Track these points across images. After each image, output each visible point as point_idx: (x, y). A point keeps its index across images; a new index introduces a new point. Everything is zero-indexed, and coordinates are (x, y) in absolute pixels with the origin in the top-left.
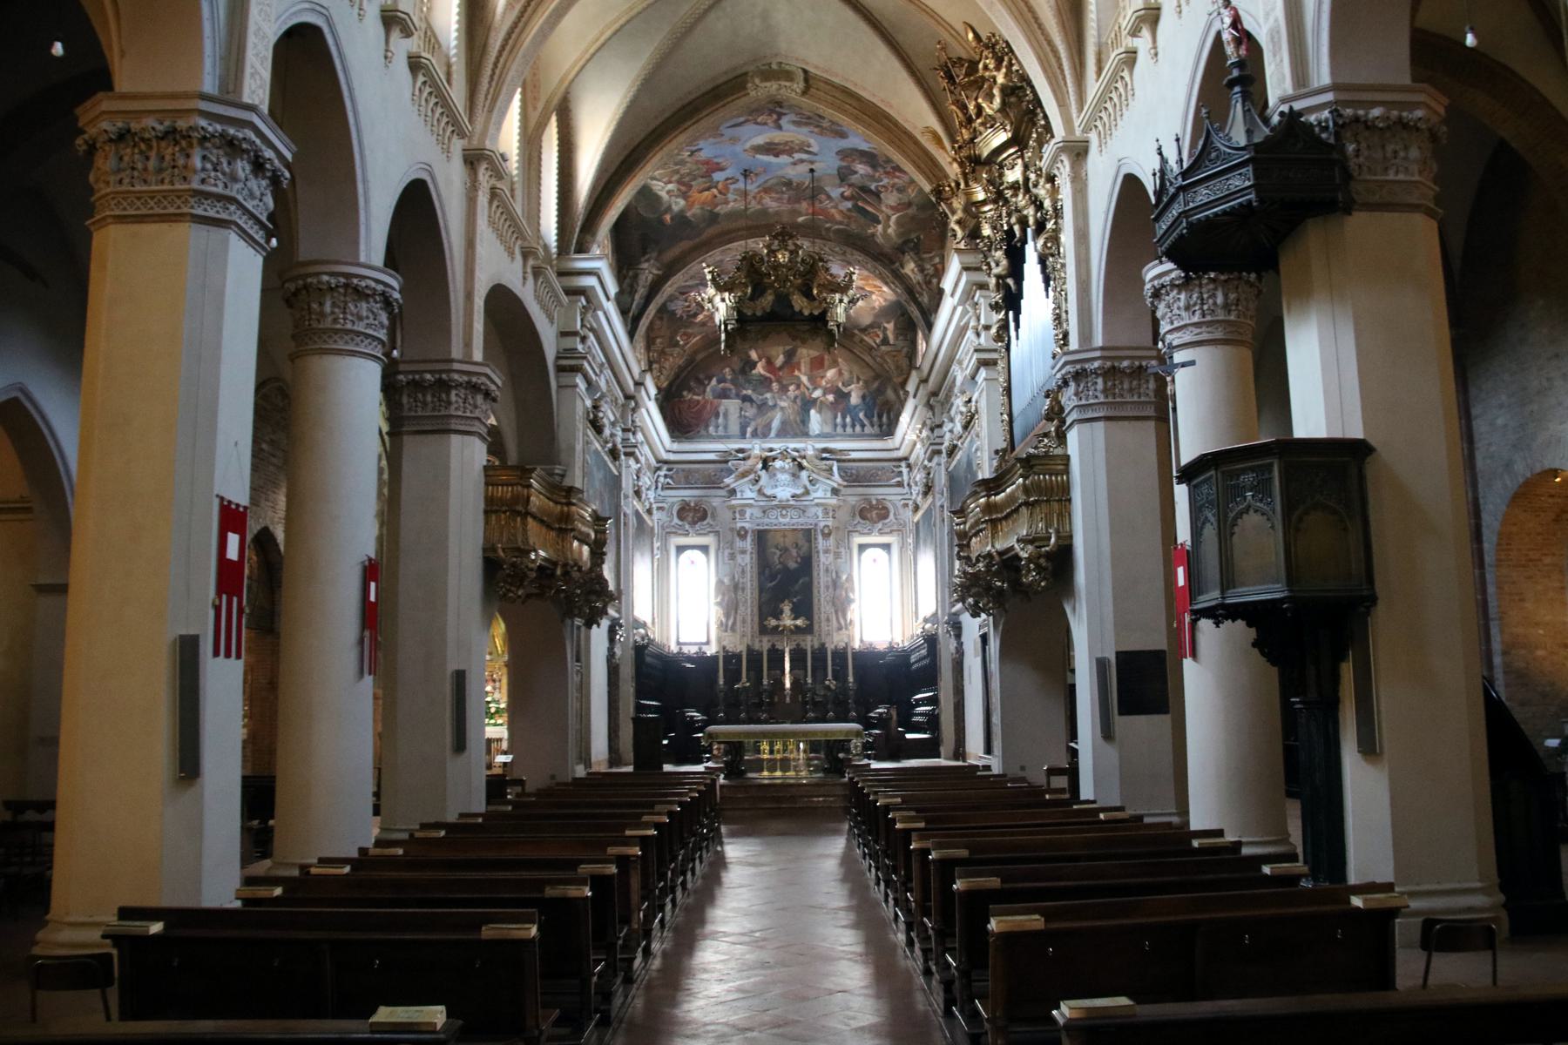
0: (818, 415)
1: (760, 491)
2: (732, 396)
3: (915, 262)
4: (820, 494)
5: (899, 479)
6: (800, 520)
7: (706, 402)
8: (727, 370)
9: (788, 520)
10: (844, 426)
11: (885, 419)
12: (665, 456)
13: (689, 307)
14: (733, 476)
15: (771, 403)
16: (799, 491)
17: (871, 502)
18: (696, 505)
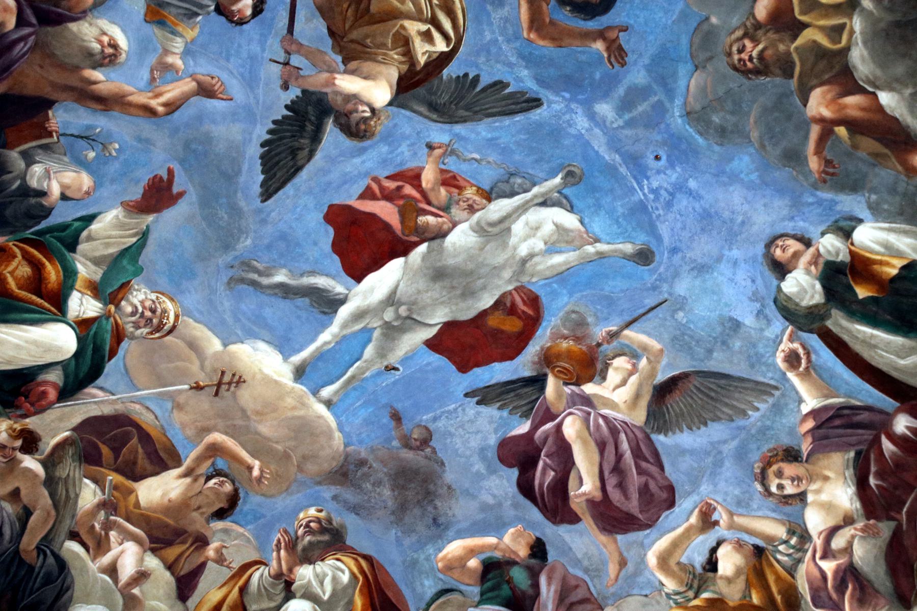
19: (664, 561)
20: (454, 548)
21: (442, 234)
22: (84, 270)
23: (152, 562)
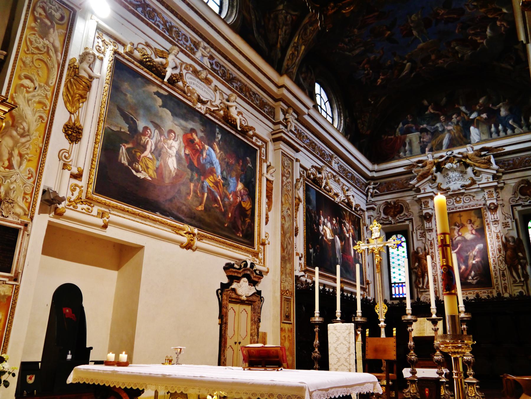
0: (476, 130)
2: (413, 131)
4: (484, 181)
7: (397, 138)
8: (409, 116)
9: (461, 204)
10: (498, 132)
12: (370, 174)
13: (368, 74)
14: (416, 179)
15: (440, 129)
16: (468, 182)
18: (395, 203)
19: (470, 9)
20: (457, 31)
21: (411, 27)
22: (400, 62)
23: (443, 59)
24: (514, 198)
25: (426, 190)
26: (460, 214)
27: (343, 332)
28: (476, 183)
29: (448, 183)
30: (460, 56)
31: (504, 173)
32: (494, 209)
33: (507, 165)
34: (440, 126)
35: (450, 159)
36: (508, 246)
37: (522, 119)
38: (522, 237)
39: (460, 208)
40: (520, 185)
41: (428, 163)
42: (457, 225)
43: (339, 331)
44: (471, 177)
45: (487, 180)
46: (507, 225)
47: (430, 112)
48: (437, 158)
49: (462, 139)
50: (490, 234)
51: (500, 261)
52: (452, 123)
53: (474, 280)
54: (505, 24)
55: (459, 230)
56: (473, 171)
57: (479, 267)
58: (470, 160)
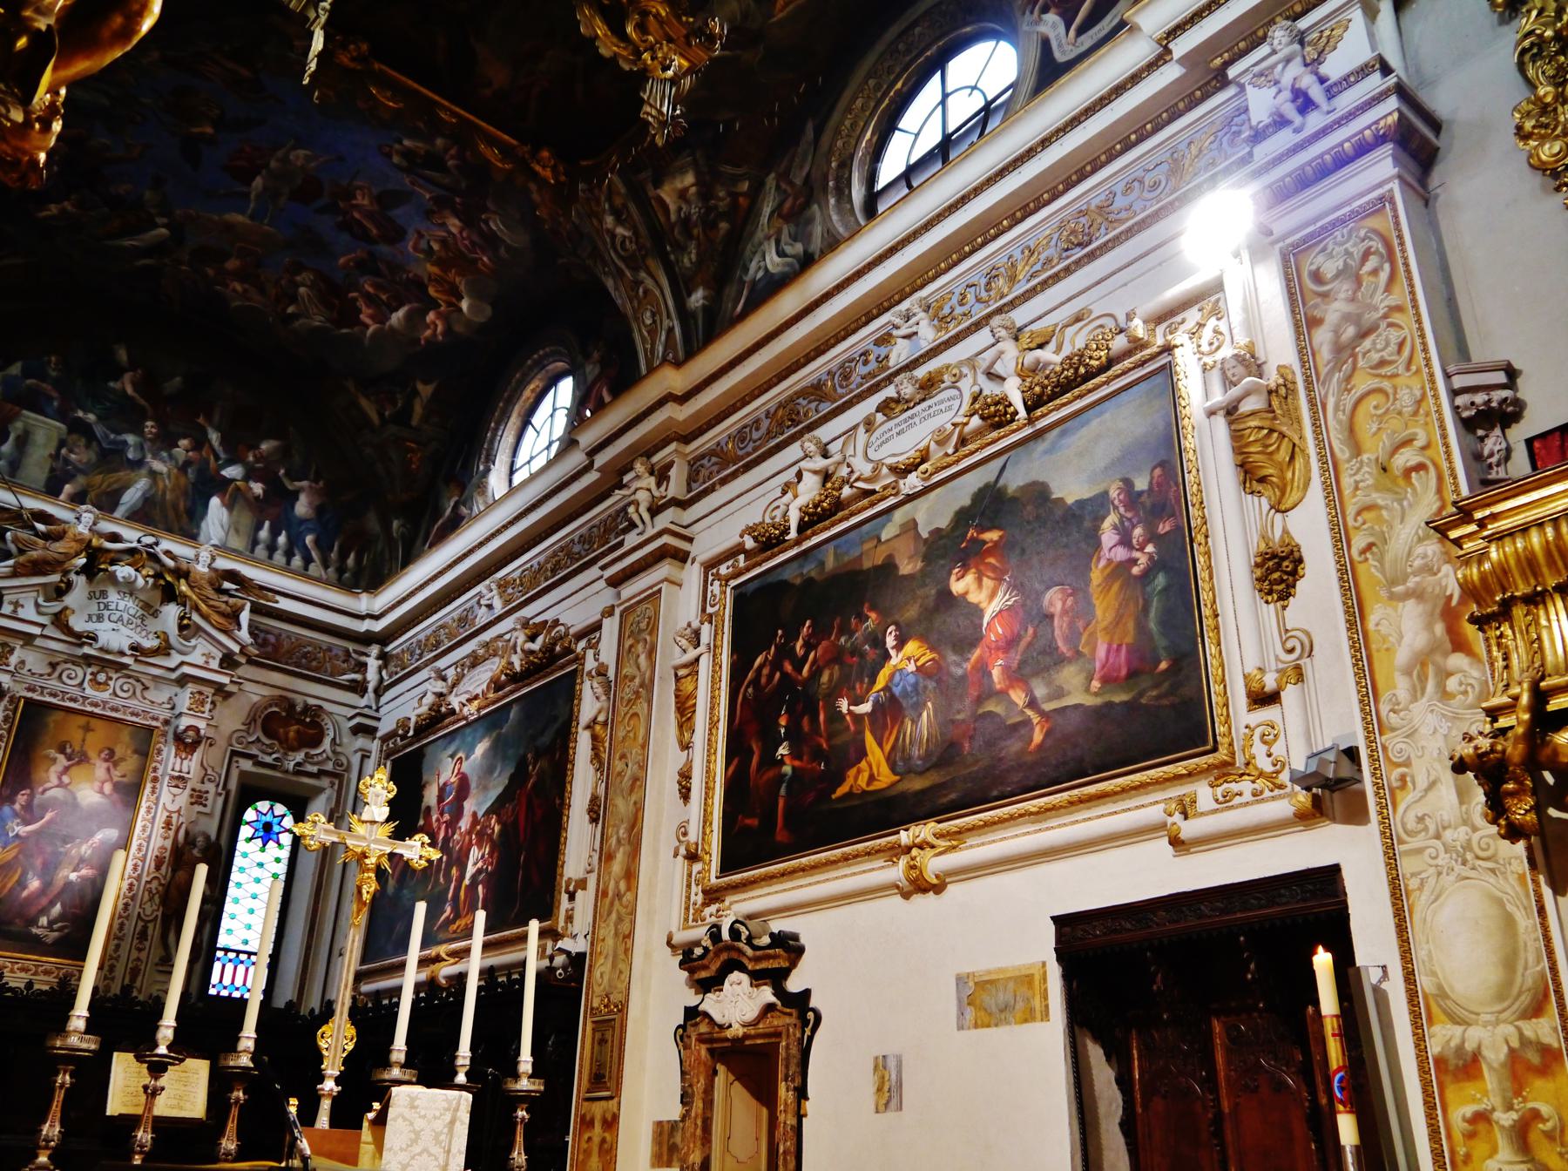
0: (224, 512)
1: (60, 620)
3: (698, 175)
4: (196, 657)
5: (358, 677)
6: (133, 703)
9: (106, 695)
10: (272, 548)
11: (351, 561)
14: (11, 562)
15: (130, 455)
16: (150, 643)
17: (291, 705)
19: (415, 248)
20: (342, 261)
22: (153, 211)
23: (246, 286)
24: (244, 734)
25: (20, 610)
26: (88, 723)
27: (435, 1118)
28: (169, 654)
29: (94, 618)
30: (290, 310)
31: (250, 662)
32: (187, 743)
33: (260, 641)
34: (135, 446)
35: (137, 556)
36: (185, 857)
37: (336, 548)
38: (224, 841)
39: (96, 705)
40: (271, 706)
41: (70, 534)
42: (69, 751)
43: (423, 1113)
44: (165, 633)
45: (204, 658)
46: (201, 797)
47: (124, 391)
48: (101, 535)
49: (178, 516)
50: (149, 808)
51: (150, 892)
52: (171, 457)
53: (52, 931)
54: (440, 329)
55: (66, 769)
56: (182, 618)
57: (82, 898)
58: (191, 587)
